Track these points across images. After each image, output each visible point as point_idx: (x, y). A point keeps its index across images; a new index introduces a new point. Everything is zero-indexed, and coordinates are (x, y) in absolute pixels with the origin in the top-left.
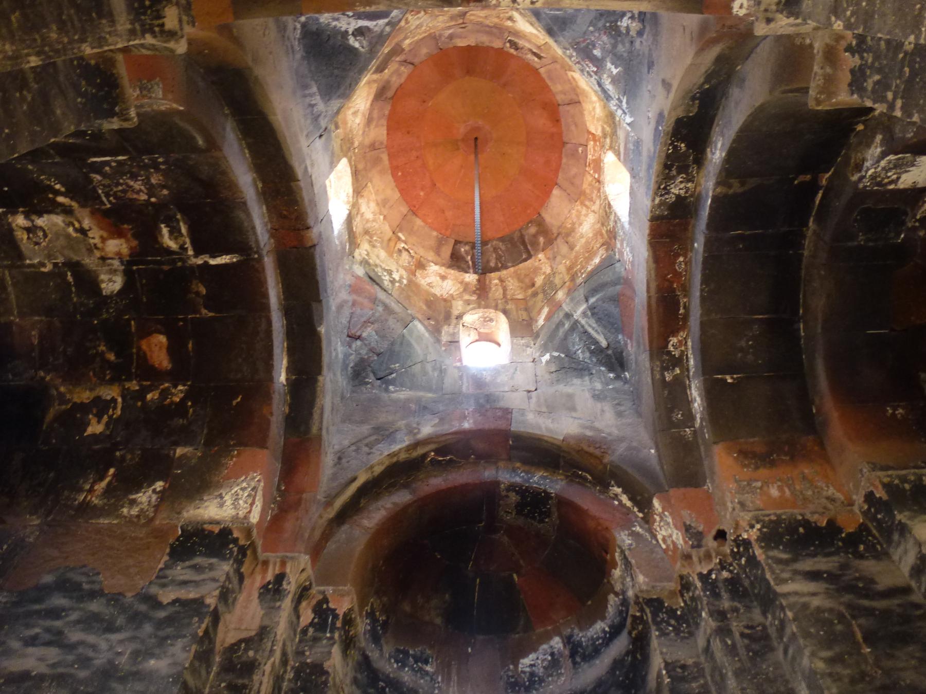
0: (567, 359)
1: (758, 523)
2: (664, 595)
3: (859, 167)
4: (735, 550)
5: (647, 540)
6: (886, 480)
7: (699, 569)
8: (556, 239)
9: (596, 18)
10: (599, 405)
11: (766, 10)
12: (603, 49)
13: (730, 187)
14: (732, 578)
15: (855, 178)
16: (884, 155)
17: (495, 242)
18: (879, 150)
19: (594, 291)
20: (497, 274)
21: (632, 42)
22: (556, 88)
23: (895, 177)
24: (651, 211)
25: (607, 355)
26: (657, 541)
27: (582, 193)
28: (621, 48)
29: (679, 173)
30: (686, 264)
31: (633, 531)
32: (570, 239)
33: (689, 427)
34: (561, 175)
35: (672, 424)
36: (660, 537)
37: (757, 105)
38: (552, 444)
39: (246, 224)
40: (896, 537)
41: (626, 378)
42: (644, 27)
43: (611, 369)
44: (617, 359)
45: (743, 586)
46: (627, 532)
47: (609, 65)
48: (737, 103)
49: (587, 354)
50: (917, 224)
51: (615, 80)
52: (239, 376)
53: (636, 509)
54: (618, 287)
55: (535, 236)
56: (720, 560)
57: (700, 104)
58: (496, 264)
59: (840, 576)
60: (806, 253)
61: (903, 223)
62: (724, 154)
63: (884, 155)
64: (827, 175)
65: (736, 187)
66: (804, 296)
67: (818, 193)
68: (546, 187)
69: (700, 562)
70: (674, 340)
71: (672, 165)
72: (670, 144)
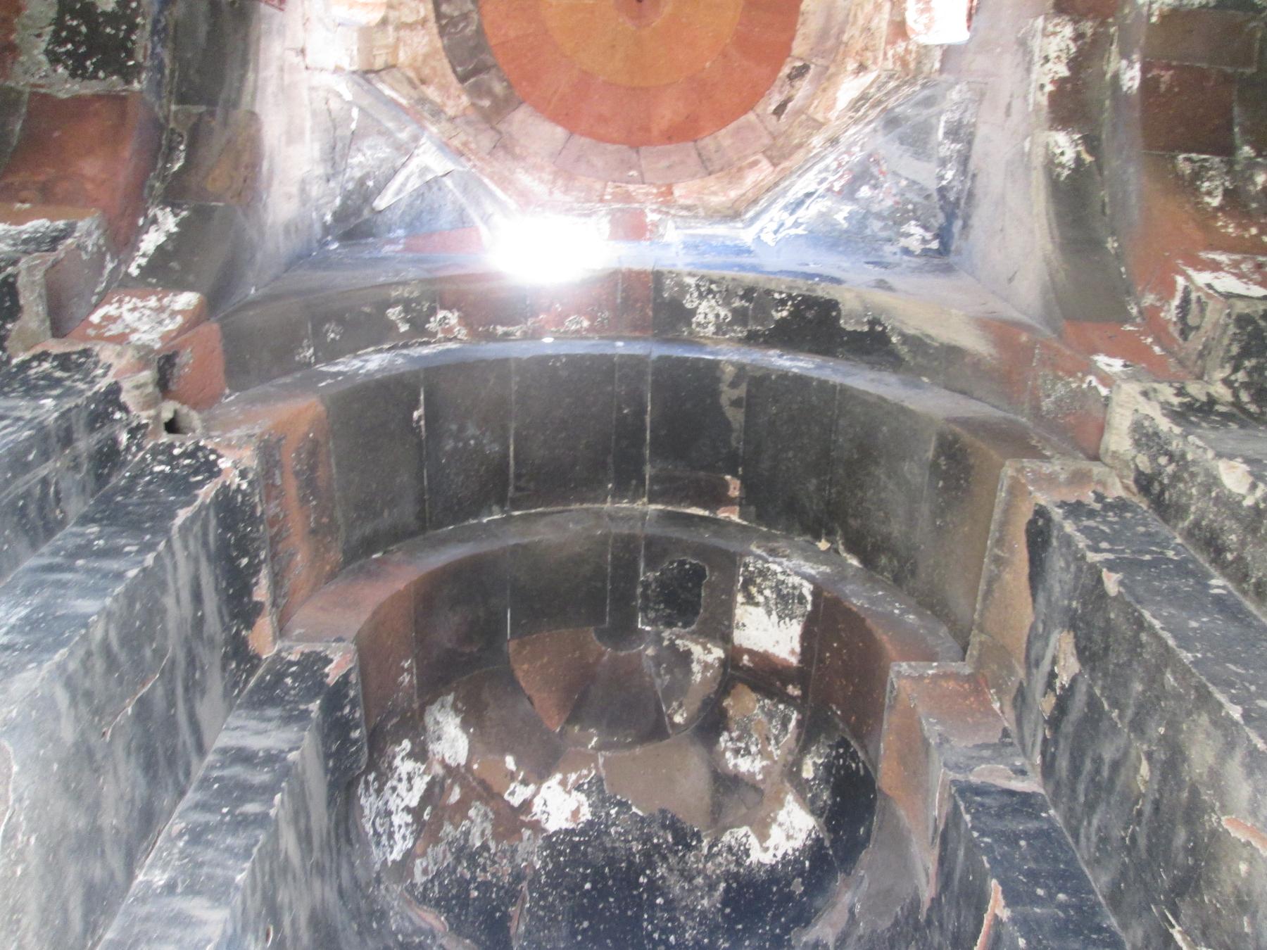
0: (349, 133)
1: (250, 483)
4: (176, 452)
5: (96, 286)
6: (353, 678)
7: (126, 385)
8: (493, 128)
9: (922, 189)
10: (294, 190)
11: (1155, 390)
12: (870, 200)
13: (733, 385)
14: (118, 453)
17: (475, 16)
18: (813, 572)
20: (432, 17)
21: (889, 240)
22: (725, 137)
23: (760, 599)
24: (670, 272)
26: (96, 306)
28: (876, 225)
29: (735, 311)
30: (577, 331)
31: (103, 256)
32: (501, 153)
33: (315, 354)
34: (585, 141)
35: (319, 322)
37: (906, 404)
38: (239, 91)
41: (326, 244)
42: (917, 256)
43: (339, 216)
44: (357, 226)
45: (109, 475)
46: (102, 242)
48: (880, 381)
49: (358, 174)
50: (666, 643)
53: (143, 261)
55: (489, 93)
56: (146, 425)
57: (861, 333)
58: (445, 16)
59: (202, 639)
60: (608, 506)
61: (670, 624)
62: (795, 370)
64: (735, 518)
65: (728, 394)
67: (705, 507)
68: (566, 115)
69: (138, 387)
70: (453, 318)
71: (750, 300)
72: (790, 297)
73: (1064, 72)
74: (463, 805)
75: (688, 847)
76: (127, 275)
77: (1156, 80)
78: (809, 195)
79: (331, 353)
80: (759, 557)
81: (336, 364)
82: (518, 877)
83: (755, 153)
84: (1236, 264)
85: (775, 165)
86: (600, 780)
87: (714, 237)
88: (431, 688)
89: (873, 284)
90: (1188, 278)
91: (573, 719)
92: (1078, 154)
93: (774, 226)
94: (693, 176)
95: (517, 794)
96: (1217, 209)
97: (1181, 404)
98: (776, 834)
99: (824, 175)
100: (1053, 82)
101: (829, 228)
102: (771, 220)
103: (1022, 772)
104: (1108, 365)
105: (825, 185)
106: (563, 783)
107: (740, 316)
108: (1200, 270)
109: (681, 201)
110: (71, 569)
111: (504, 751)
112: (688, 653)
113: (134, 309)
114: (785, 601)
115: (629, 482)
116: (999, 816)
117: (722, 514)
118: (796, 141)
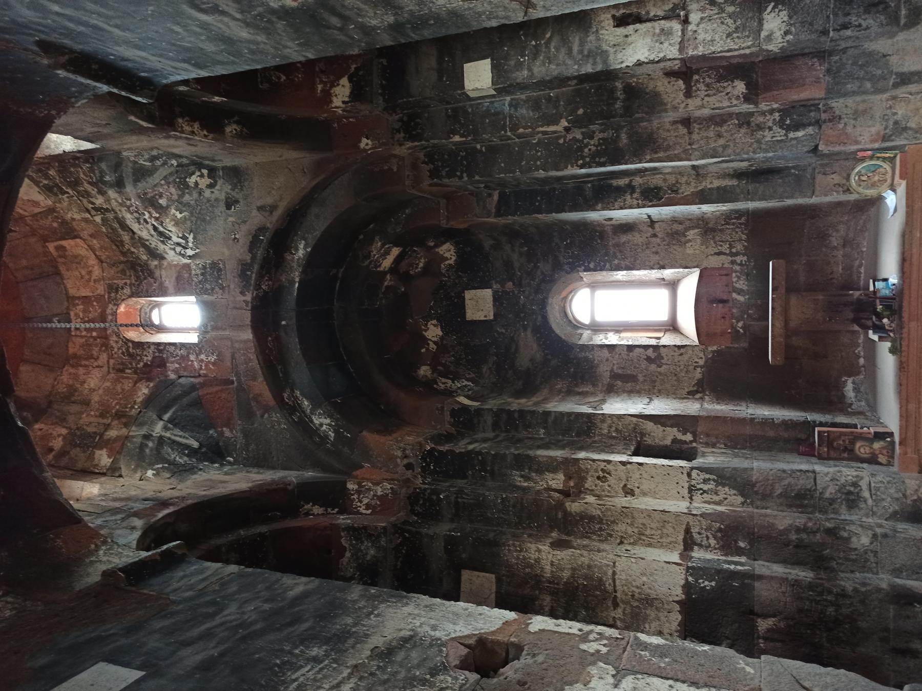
3: (368, 256)
12: (169, 199)
15: (367, 263)
18: (379, 244)
21: (200, 193)
25: (203, 453)
27: (75, 356)
28: (187, 198)
36: (362, 510)
40: (476, 421)
42: (216, 182)
47: (173, 211)
49: (186, 458)
51: (177, 223)
53: (329, 510)
62: (309, 250)
63: (383, 245)
76: (338, 513)
78: (155, 229)
80: (370, 263)
83: (45, 247)
84: (321, 82)
86: (423, 318)
87: (179, 278)
89: (267, 214)
90: (336, 107)
92: (235, 122)
93: (178, 249)
95: (432, 346)
96: (287, 78)
97: (404, 133)
98: (447, 255)
99: (142, 221)
100: (202, 130)
101: (189, 222)
102: (174, 249)
103: (490, 195)
104: (367, 144)
106: (426, 331)
108: (331, 102)
109: (101, 289)
112: (387, 287)
113: (361, 502)
117: (340, 275)
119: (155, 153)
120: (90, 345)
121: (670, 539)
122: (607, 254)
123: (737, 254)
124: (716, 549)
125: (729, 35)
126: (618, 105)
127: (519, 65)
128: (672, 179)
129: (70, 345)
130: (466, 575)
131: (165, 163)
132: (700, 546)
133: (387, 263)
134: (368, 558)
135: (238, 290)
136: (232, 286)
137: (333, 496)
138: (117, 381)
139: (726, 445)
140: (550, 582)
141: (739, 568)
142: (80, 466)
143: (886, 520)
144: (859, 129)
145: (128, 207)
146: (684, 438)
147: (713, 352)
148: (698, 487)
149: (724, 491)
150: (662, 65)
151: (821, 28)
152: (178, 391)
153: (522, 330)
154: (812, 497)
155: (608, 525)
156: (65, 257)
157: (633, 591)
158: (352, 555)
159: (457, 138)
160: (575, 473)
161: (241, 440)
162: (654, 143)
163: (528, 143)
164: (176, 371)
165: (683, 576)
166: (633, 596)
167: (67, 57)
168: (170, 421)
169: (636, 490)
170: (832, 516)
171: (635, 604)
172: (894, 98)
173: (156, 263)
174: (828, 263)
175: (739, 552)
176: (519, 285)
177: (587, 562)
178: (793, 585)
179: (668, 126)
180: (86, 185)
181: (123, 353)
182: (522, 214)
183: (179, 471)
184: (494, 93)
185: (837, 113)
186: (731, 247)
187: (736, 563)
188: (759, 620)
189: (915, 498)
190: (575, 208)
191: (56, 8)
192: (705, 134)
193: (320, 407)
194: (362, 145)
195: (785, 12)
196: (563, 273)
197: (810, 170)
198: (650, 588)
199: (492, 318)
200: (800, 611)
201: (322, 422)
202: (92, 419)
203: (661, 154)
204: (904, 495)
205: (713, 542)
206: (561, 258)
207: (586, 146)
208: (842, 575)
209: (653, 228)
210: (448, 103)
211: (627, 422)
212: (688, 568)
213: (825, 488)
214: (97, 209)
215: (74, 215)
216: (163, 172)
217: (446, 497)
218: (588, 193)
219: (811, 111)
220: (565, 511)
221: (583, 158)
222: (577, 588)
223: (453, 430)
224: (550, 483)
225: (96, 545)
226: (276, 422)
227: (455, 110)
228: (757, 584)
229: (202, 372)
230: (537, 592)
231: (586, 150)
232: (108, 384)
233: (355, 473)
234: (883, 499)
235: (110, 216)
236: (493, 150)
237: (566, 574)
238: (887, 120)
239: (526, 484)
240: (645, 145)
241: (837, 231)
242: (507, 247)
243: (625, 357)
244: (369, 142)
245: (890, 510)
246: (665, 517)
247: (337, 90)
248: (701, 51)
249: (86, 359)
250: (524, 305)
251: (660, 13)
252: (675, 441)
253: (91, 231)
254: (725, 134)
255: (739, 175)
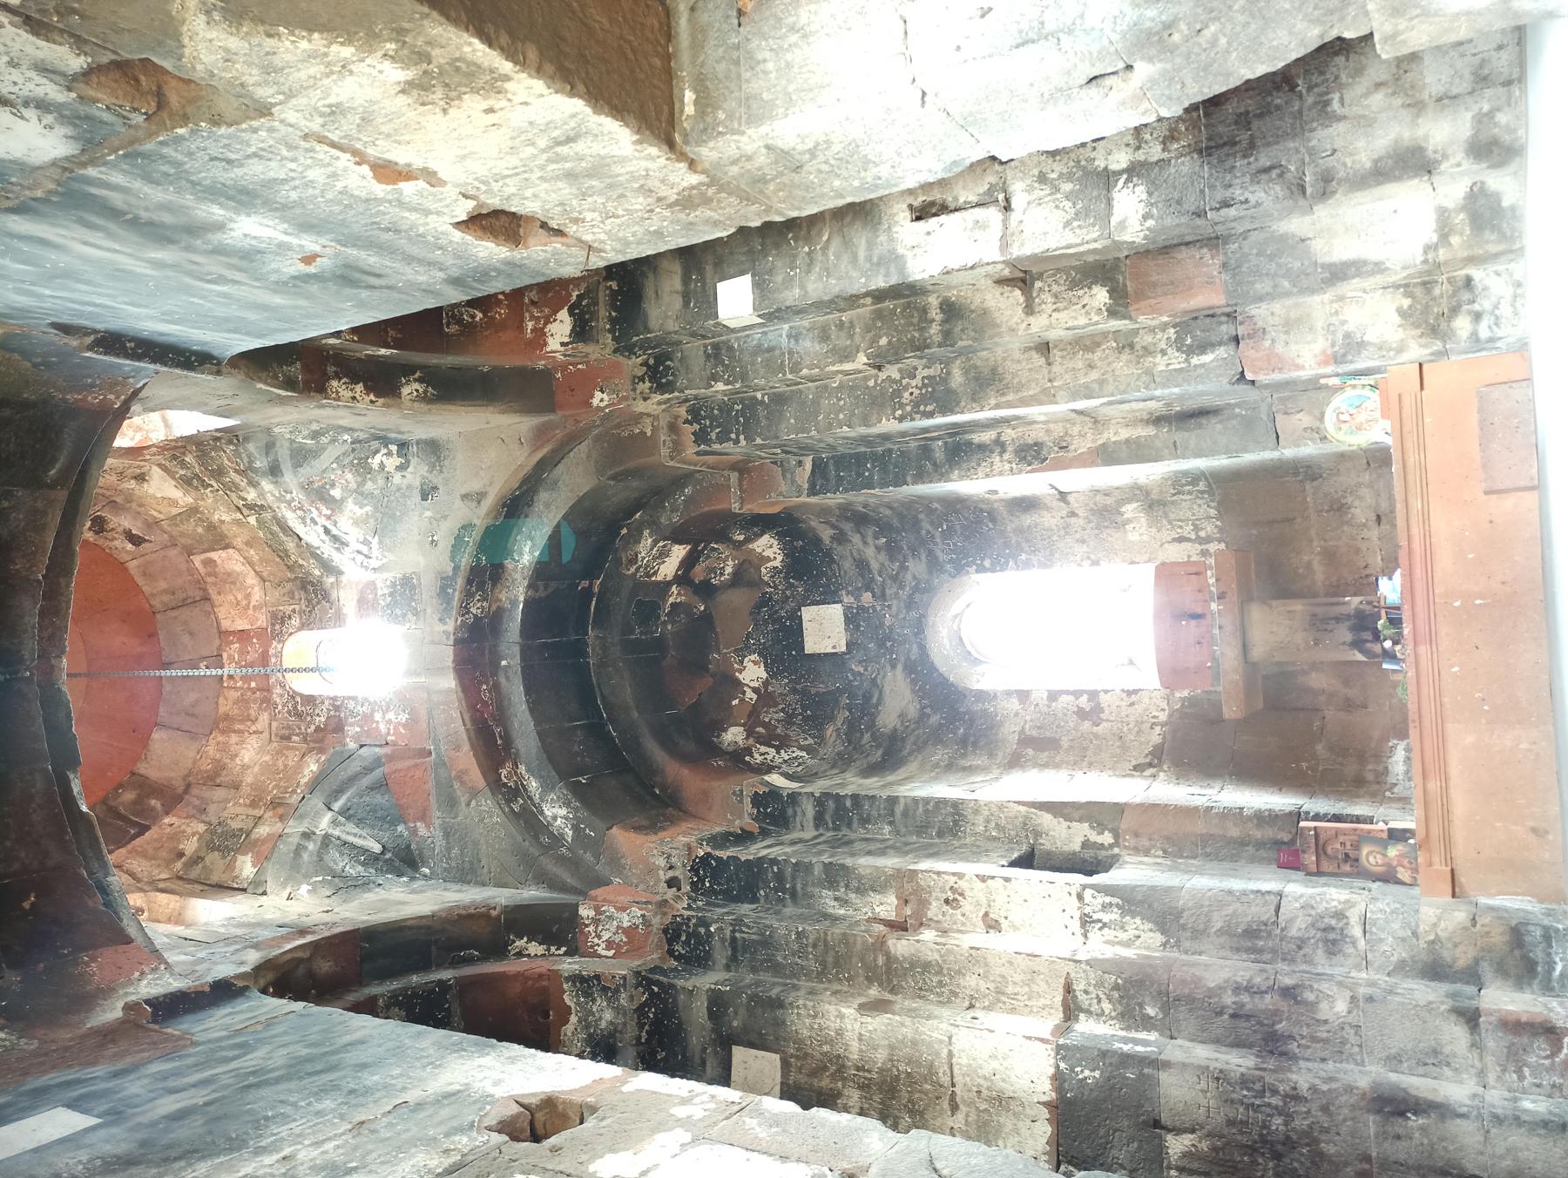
2: (658, 963)
3: (633, 561)
8: (186, 791)
12: (345, 489)
15: (632, 570)
16: (655, 543)
19: (338, 792)
27: (227, 717)
28: (369, 485)
38: (420, 928)
39: (27, 619)
40: (790, 812)
42: (408, 462)
49: (360, 868)
52: (16, 866)
53: (553, 949)
54: (378, 773)
63: (655, 543)
65: (542, 594)
66: (604, 698)
73: (359, 387)
74: (764, 725)
75: (770, 599)
76: (566, 954)
77: (394, 340)
78: (327, 531)
79: (558, 839)
80: (637, 570)
81: (562, 836)
82: (794, 691)
84: (532, 318)
85: (227, 547)
87: (362, 602)
88: (716, 750)
91: (707, 670)
93: (360, 558)
94: (211, 613)
95: (750, 695)
96: (485, 315)
98: (769, 553)
103: (800, 463)
105: (322, 521)
107: (481, 586)
108: (545, 344)
109: (262, 620)
110: (794, 888)
111: (732, 707)
113: (599, 937)
114: (664, 554)
115: (579, 649)
116: (828, 480)
118: (200, 530)
119: (315, 427)
120: (247, 701)
121: (1042, 1001)
122: (1007, 545)
123: (1208, 540)
124: (1112, 1018)
125: (1067, 224)
126: (934, 329)
127: (789, 282)
128: (1058, 430)
129: (221, 700)
130: (739, 1053)
131: (333, 441)
132: (1089, 1012)
133: (668, 568)
134: (603, 1024)
135: (436, 618)
136: (429, 611)
137: (556, 927)
138: (279, 753)
139: (1165, 852)
140: (858, 1069)
141: (1139, 1048)
142: (215, 879)
143: (1389, 975)
144: (1293, 347)
145: (289, 503)
146: (1099, 839)
147: (1183, 699)
148: (1095, 917)
149: (1135, 924)
150: (982, 271)
151: (1193, 208)
152: (354, 767)
153: (888, 668)
154: (1269, 933)
155: (951, 978)
156: (215, 575)
157: (979, 1085)
158: (579, 1022)
159: (720, 386)
160: (912, 893)
161: (440, 843)
162: (1000, 381)
163: (826, 387)
164: (356, 738)
165: (1052, 1061)
166: (979, 1092)
167: (92, 337)
168: (341, 813)
169: (1002, 921)
170: (1304, 967)
171: (983, 1106)
172: (1341, 298)
173: (332, 579)
174: (1358, 551)
175: (1147, 1023)
176: (883, 596)
177: (910, 1036)
178: (1218, 1079)
179: (1017, 355)
180: (232, 474)
181: (289, 712)
182: (846, 490)
183: (345, 886)
184: (760, 321)
185: (1260, 324)
186: (1196, 528)
187: (1136, 1042)
188: (1169, 1137)
189: (1432, 937)
190: (920, 477)
191: (47, 292)
192: (1071, 365)
193: (552, 789)
194: (595, 402)
195: (1142, 188)
196: (945, 577)
197: (1264, 408)
198: (1004, 1080)
199: (844, 649)
200: (1231, 1123)
201: (557, 813)
202: (239, 810)
203: (1010, 397)
204: (1415, 934)
205: (1107, 1006)
206: (939, 554)
207: (906, 388)
208: (1302, 1064)
209: (1067, 503)
210: (704, 337)
211: (1012, 814)
212: (1059, 1048)
213: (1291, 921)
214: (251, 507)
215: (223, 515)
216: (333, 452)
217: (720, 929)
218: (939, 455)
219: (1221, 323)
220: (888, 954)
221: (902, 406)
222: (897, 1078)
223: (754, 827)
224: (877, 910)
225: (142, 973)
226: (485, 815)
227: (716, 347)
228: (1164, 1077)
229: (390, 738)
230: (840, 1084)
231: (906, 395)
232: (267, 758)
233: (593, 893)
234: (1381, 940)
235: (267, 515)
236: (779, 400)
237: (881, 1056)
238: (1334, 333)
239: (842, 912)
240: (986, 382)
241: (1361, 498)
242: (856, 539)
243: (1046, 709)
244: (605, 396)
245: (1394, 959)
246: (1035, 964)
247: (553, 328)
248: (1027, 251)
249: (241, 722)
250: (891, 628)
251: (973, 198)
252: (1086, 844)
253: (246, 538)
254: (1099, 364)
255: (1158, 420)
